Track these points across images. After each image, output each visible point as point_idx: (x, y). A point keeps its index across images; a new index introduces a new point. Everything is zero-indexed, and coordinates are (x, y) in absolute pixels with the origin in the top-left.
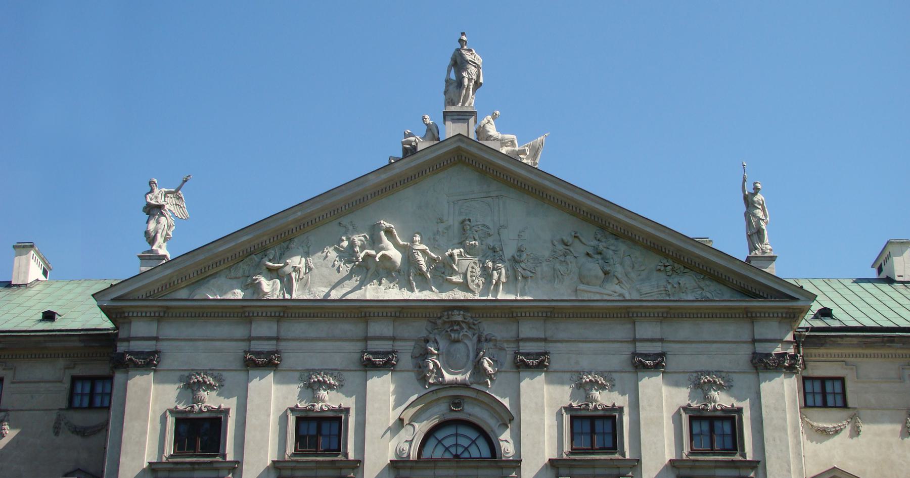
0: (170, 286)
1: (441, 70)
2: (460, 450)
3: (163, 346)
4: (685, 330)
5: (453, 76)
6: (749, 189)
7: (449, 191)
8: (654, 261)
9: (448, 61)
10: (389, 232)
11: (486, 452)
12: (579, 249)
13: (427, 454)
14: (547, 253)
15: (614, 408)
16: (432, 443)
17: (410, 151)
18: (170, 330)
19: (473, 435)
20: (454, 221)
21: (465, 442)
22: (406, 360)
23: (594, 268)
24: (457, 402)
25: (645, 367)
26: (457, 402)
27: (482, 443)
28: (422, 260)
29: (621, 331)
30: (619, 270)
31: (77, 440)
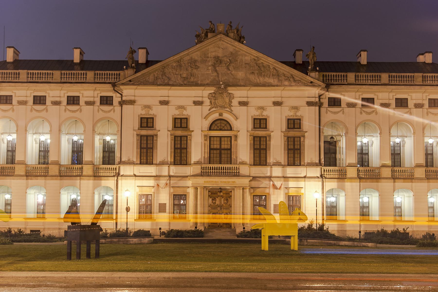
2: (222, 127)
11: (229, 128)
21: (223, 125)
24: (221, 115)
26: (221, 115)
27: (228, 125)
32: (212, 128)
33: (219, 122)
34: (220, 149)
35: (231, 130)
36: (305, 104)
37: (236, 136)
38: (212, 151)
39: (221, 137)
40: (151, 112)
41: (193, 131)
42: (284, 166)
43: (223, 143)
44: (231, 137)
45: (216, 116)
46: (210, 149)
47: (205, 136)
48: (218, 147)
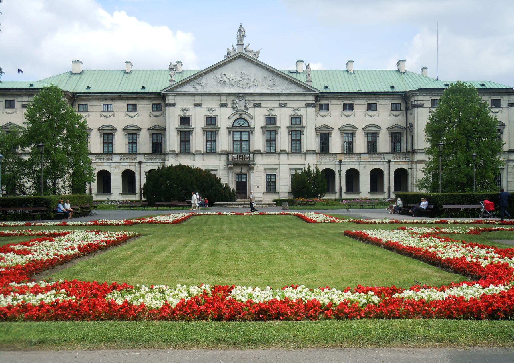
0: (176, 87)
1: (236, 33)
3: (176, 101)
4: (291, 98)
5: (239, 34)
6: (307, 64)
7: (240, 63)
8: (285, 82)
9: (237, 31)
10: (225, 75)
11: (247, 125)
12: (268, 79)
13: (234, 125)
14: (261, 80)
15: (275, 115)
16: (235, 123)
17: (229, 53)
18: (177, 98)
19: (244, 121)
20: (240, 72)
22: (229, 105)
23: (271, 83)
24: (241, 114)
25: (283, 106)
26: (241, 114)
28: (233, 82)
29: (277, 98)
30: (277, 84)
31: (155, 118)
32: (234, 125)
33: (239, 120)
34: (241, 141)
35: (249, 127)
36: (304, 105)
37: (252, 132)
38: (234, 143)
39: (241, 132)
40: (188, 113)
41: (220, 128)
42: (288, 153)
43: (242, 136)
44: (249, 131)
45: (237, 116)
46: (233, 141)
47: (230, 132)
48: (239, 139)
